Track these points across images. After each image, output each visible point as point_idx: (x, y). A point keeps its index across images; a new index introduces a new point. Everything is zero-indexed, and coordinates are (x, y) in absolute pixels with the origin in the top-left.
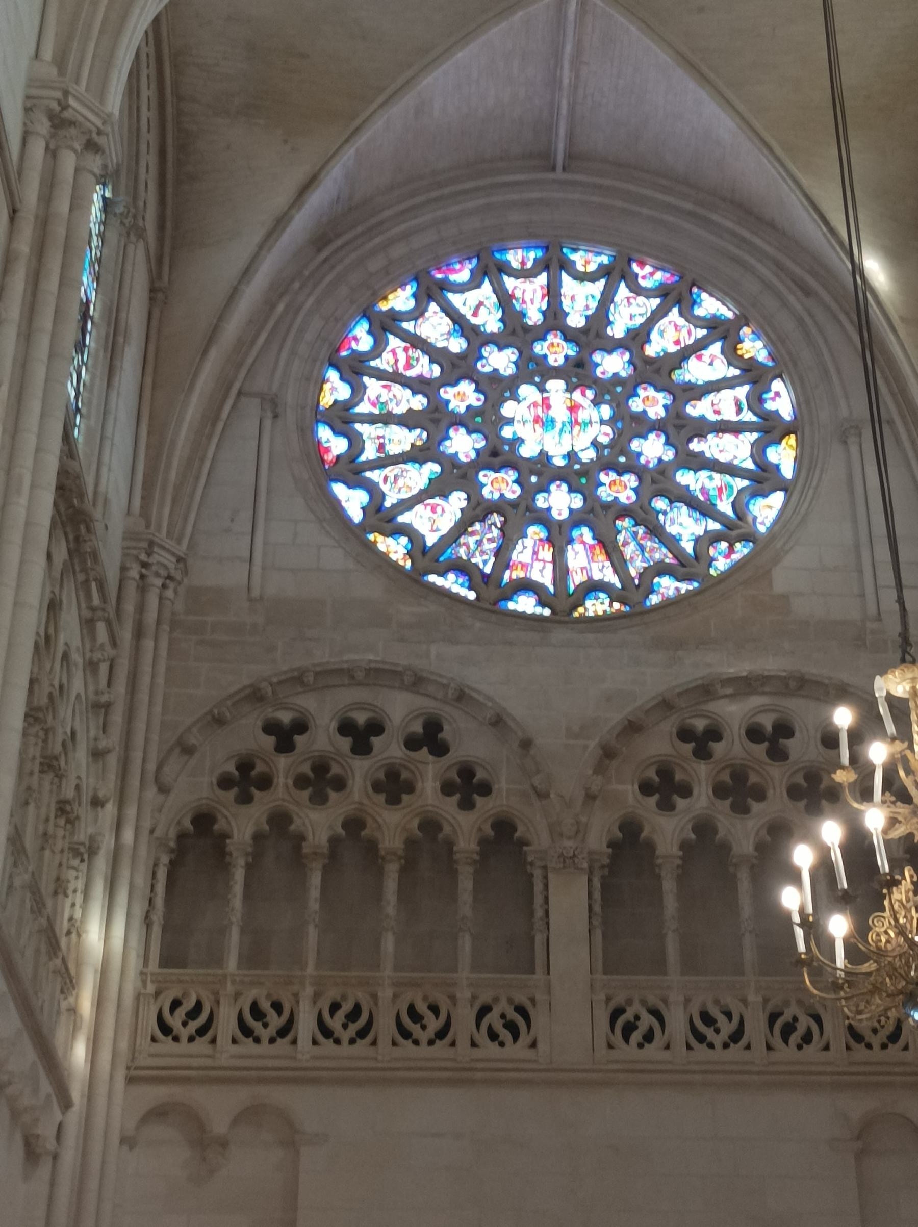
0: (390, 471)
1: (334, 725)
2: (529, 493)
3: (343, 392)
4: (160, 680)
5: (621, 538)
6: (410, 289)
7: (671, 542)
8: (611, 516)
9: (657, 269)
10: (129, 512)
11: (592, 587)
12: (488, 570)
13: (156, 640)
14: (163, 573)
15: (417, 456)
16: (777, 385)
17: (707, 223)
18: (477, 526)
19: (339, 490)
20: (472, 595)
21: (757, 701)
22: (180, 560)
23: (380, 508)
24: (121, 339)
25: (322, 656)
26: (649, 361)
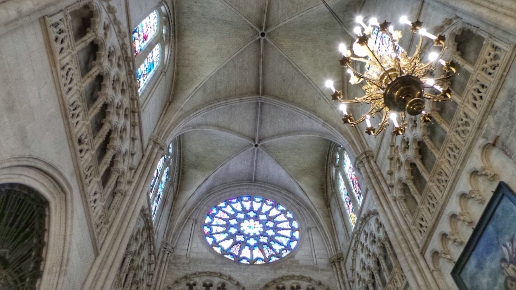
0: (218, 235)
1: (202, 284)
2: (246, 240)
3: (210, 220)
4: (165, 273)
5: (264, 249)
6: (224, 203)
7: (274, 250)
8: (262, 244)
9: (271, 201)
10: (163, 237)
11: (258, 259)
12: (237, 254)
13: (165, 265)
14: (169, 250)
15: (224, 232)
16: (294, 222)
17: (280, 193)
18: (235, 246)
19: (208, 238)
20: (233, 259)
21: (293, 281)
22: (173, 248)
23: (215, 242)
24: (166, 203)
25: (200, 270)
26: (269, 217)
